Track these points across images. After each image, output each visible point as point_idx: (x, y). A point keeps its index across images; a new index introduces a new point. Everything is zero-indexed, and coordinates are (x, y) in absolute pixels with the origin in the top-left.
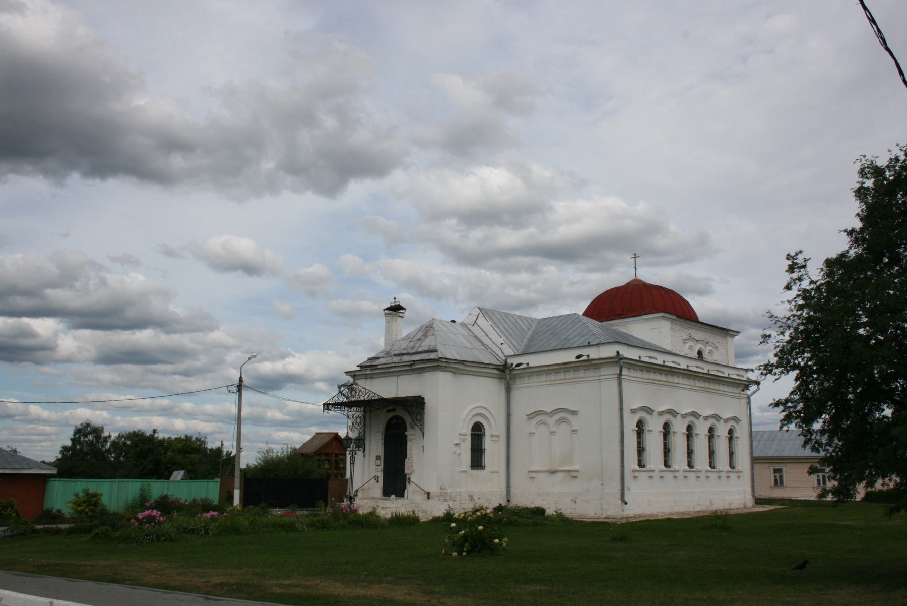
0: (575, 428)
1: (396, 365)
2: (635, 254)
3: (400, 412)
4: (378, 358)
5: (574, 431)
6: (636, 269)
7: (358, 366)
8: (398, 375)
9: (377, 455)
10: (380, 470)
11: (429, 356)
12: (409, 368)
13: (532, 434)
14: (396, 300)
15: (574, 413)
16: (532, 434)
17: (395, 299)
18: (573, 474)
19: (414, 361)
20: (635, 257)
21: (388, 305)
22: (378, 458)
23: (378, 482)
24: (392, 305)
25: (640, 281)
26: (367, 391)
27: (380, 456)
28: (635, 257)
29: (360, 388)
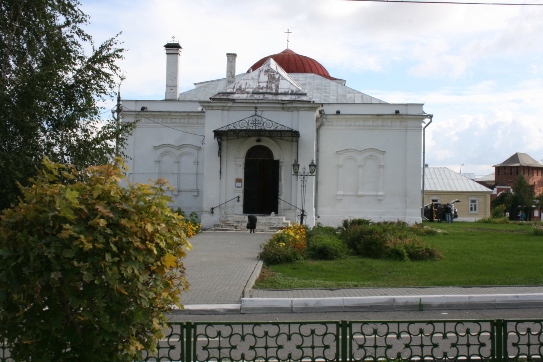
0: (382, 164)
1: (260, 101)
2: (288, 30)
3: (267, 143)
4: (233, 93)
5: (381, 167)
6: (288, 40)
7: (210, 98)
8: (263, 111)
9: (236, 178)
10: (242, 191)
11: (298, 98)
12: (282, 106)
13: (339, 166)
14: (174, 39)
15: (384, 152)
16: (339, 166)
17: (173, 37)
18: (379, 198)
19: (282, 100)
20: (288, 32)
21: (166, 44)
22: (238, 180)
23: (238, 201)
24: (169, 42)
25: (291, 51)
26: (274, 123)
27: (241, 179)
28: (288, 32)
29: (264, 120)
